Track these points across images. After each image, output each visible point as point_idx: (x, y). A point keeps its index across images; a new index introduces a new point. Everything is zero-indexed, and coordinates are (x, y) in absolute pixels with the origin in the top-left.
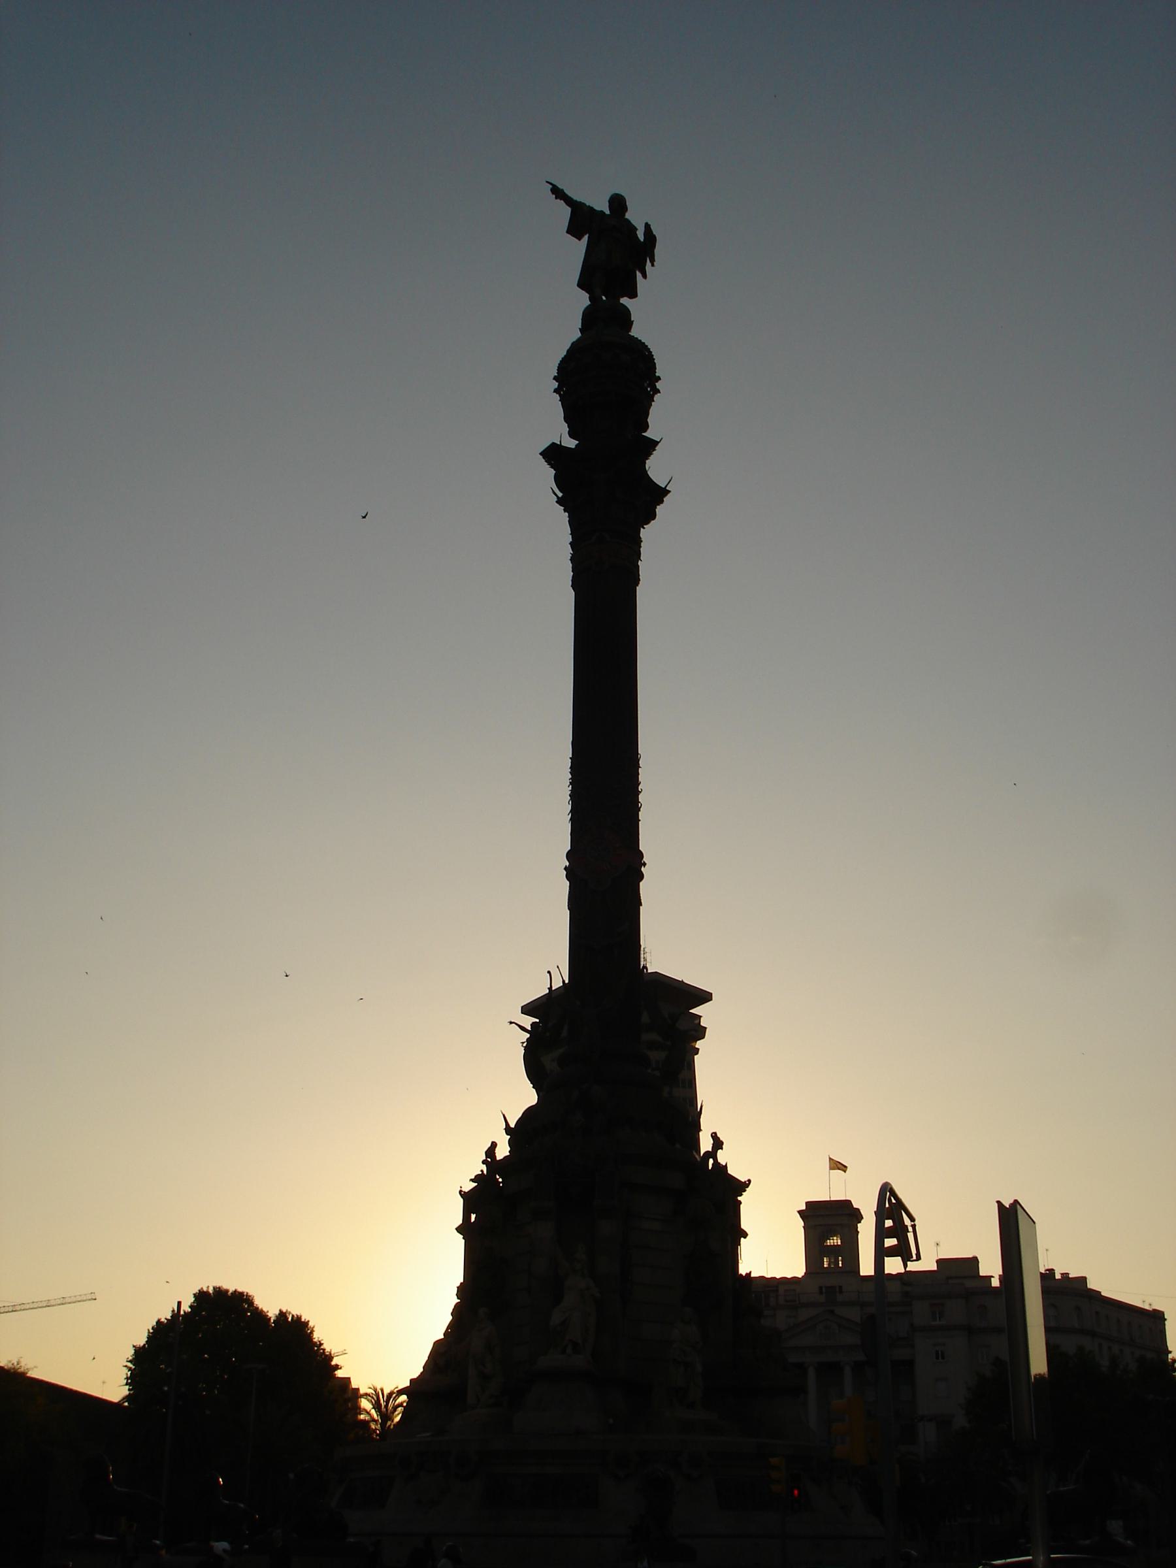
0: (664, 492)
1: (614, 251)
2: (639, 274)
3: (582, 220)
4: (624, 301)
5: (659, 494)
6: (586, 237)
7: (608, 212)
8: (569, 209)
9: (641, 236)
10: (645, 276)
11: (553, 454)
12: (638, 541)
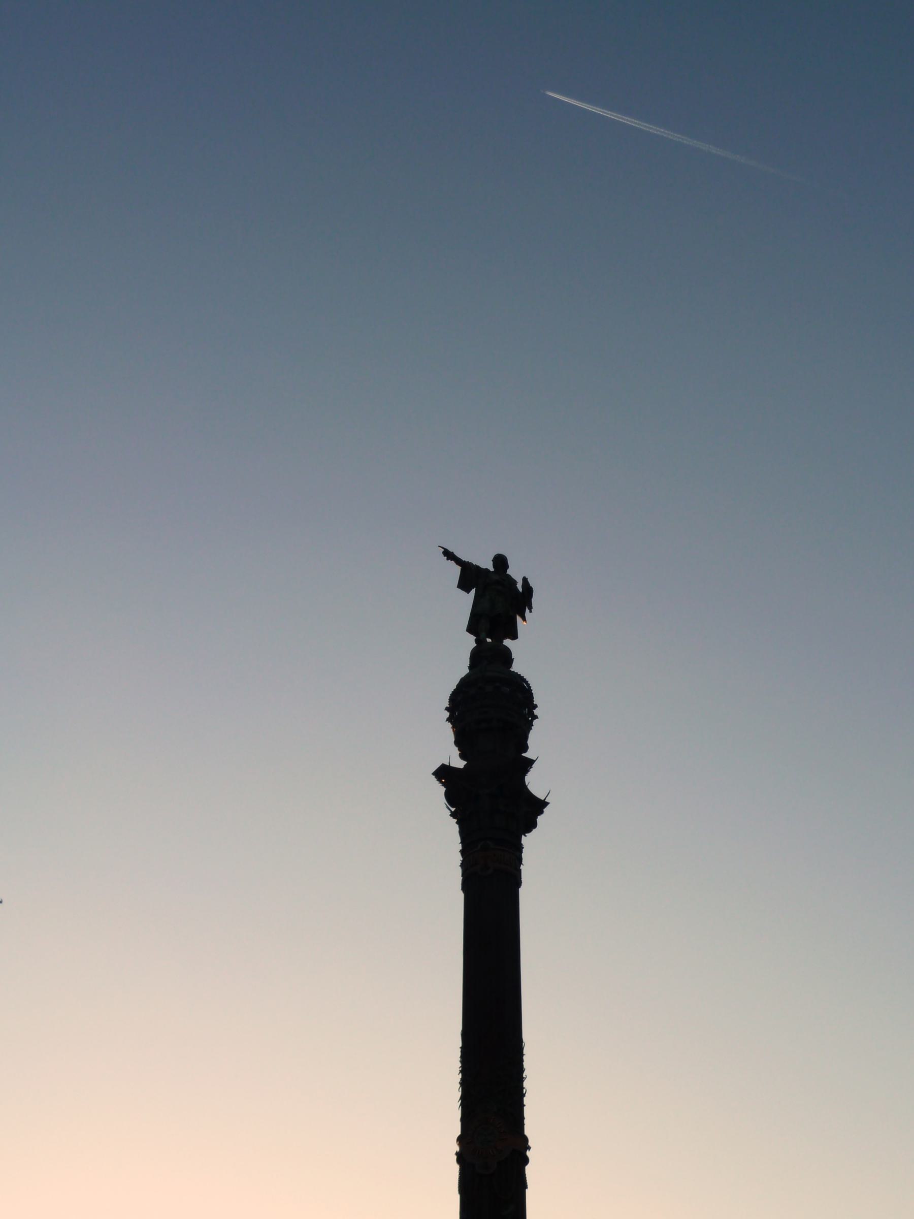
0: (544, 804)
1: (497, 600)
2: (519, 619)
3: (470, 577)
4: (507, 642)
5: (540, 805)
6: (473, 591)
7: (492, 569)
8: (458, 569)
9: (519, 586)
10: (524, 619)
11: (443, 773)
12: (519, 848)
